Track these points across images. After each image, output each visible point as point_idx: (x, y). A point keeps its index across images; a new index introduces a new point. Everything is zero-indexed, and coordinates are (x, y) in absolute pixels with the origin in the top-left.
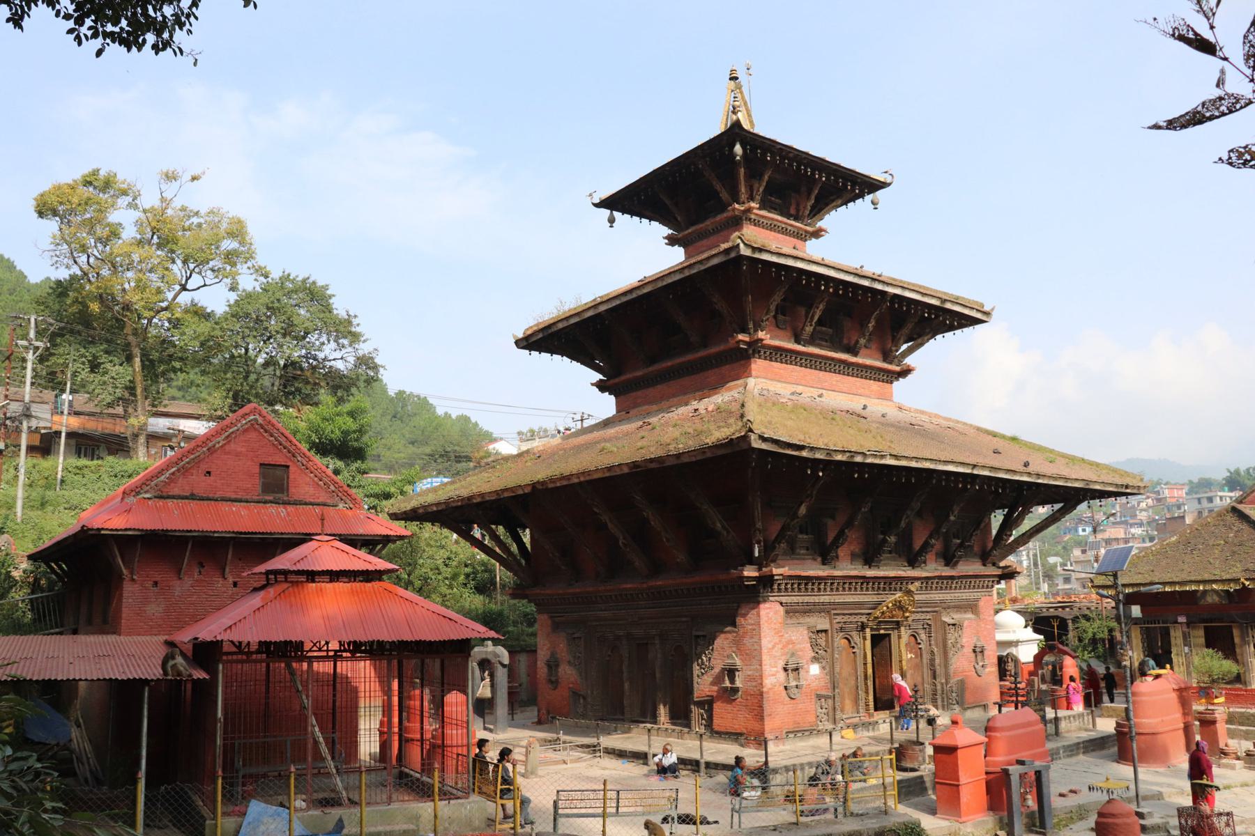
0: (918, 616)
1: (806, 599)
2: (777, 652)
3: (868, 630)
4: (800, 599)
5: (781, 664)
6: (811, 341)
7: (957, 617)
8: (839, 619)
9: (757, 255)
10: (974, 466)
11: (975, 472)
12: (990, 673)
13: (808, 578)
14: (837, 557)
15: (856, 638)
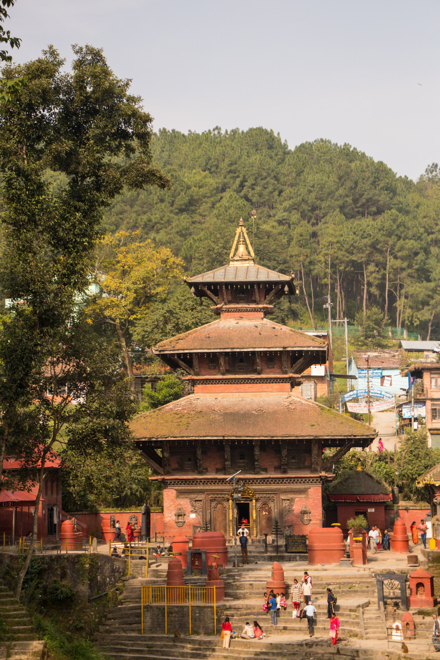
0: (264, 495)
1: (189, 488)
2: (172, 508)
3: (230, 501)
4: (186, 488)
5: (174, 513)
6: (228, 372)
7: (290, 496)
8: (211, 496)
9: (162, 353)
10: (223, 437)
11: (226, 438)
12: (315, 524)
13: (186, 480)
14: (206, 469)
15: (225, 504)
